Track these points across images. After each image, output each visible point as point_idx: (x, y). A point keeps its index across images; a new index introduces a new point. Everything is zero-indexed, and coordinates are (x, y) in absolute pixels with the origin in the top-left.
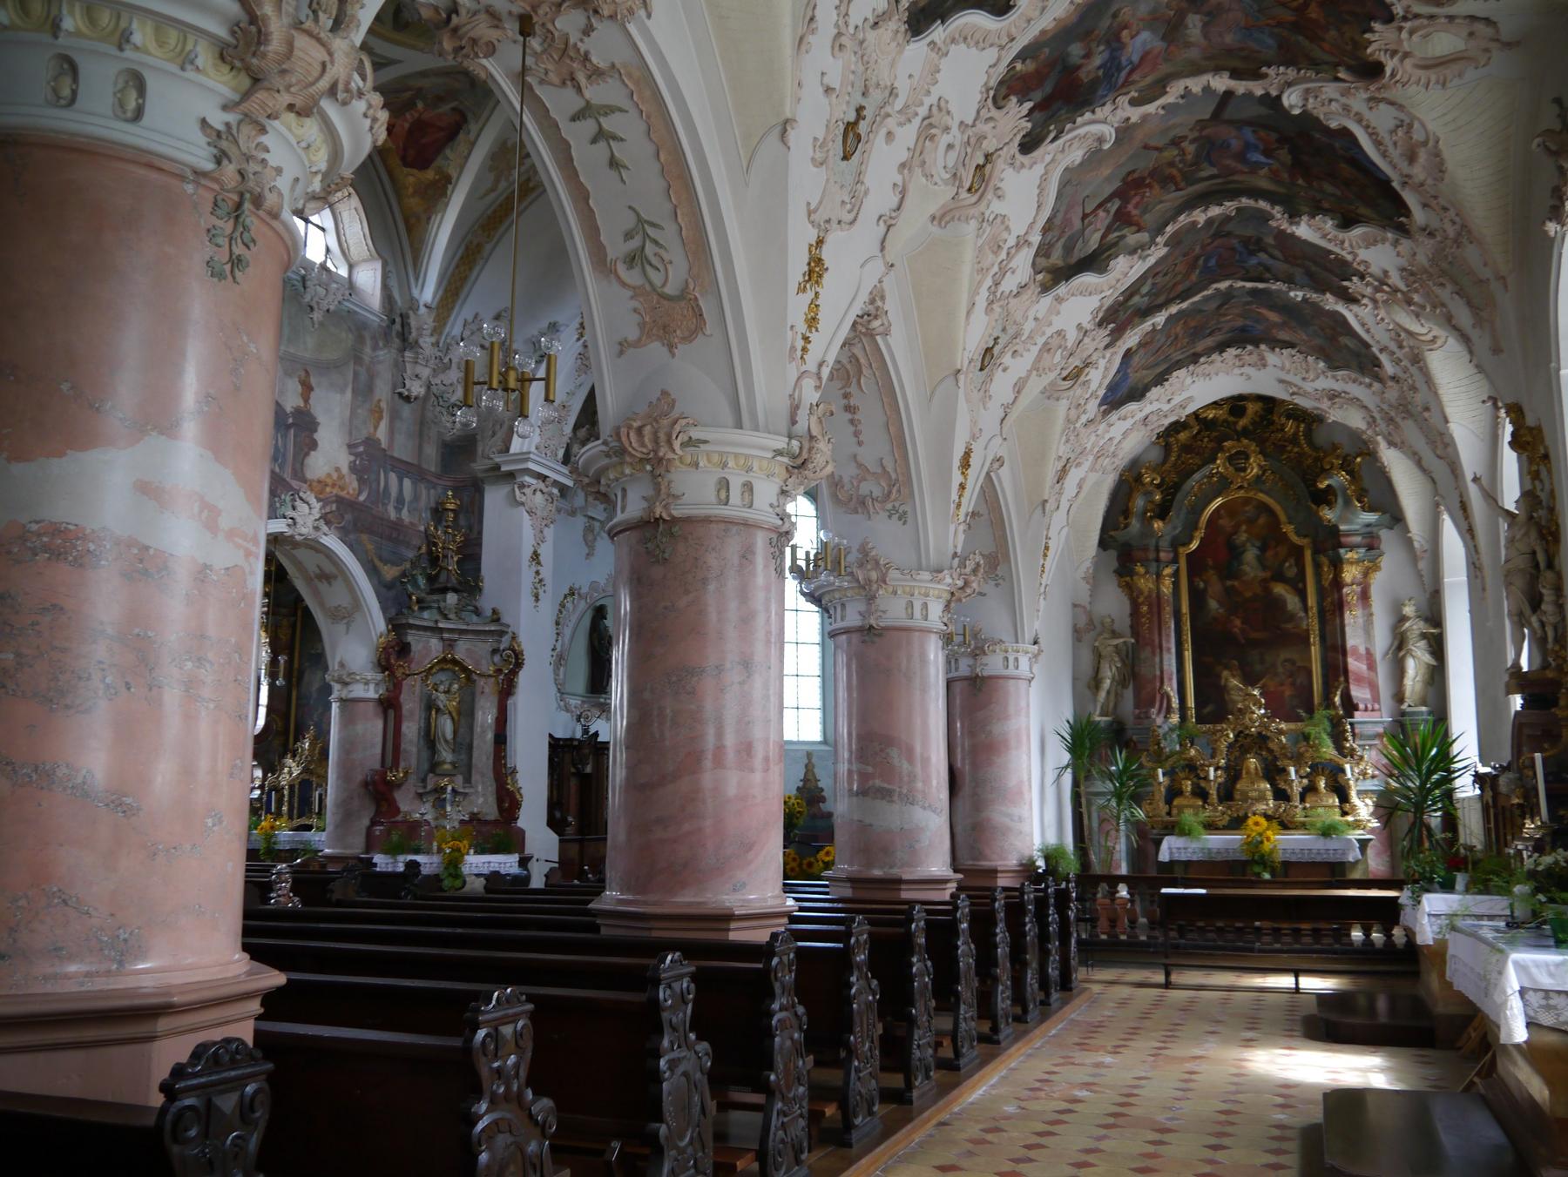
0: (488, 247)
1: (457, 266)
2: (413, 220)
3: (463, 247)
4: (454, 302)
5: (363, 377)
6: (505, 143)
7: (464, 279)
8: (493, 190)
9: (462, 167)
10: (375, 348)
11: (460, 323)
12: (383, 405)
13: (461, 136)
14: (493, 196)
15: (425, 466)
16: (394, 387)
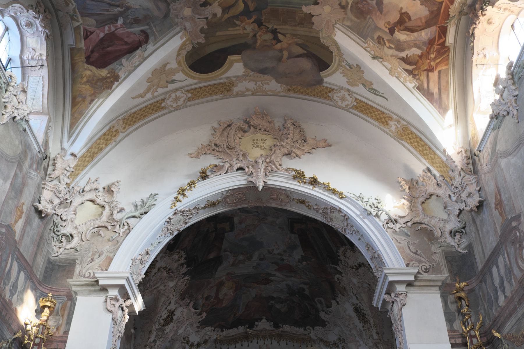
0: (121, 135)
1: (100, 139)
2: (79, 99)
3: (108, 128)
4: (89, 162)
5: (19, 180)
6: (165, 65)
7: (101, 149)
8: (141, 96)
9: (130, 73)
10: (31, 166)
11: (86, 179)
12: (25, 208)
13: (138, 52)
14: (141, 100)
15: (35, 270)
16: (34, 201)
